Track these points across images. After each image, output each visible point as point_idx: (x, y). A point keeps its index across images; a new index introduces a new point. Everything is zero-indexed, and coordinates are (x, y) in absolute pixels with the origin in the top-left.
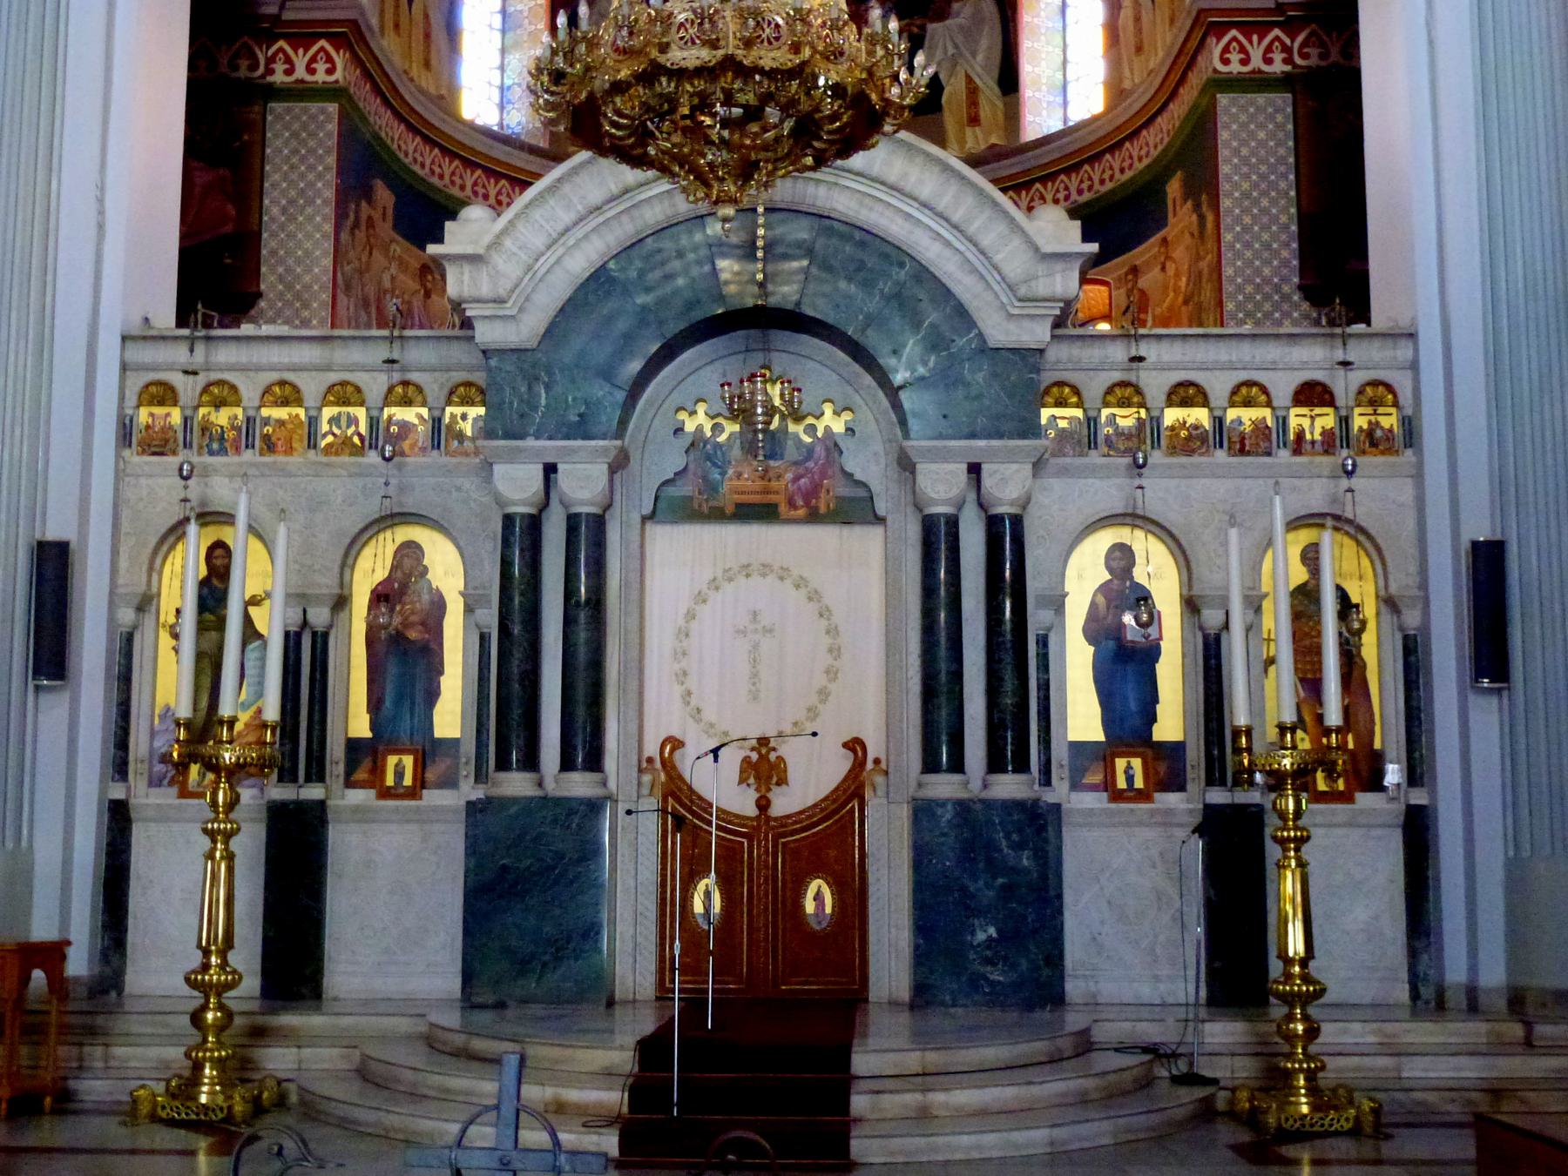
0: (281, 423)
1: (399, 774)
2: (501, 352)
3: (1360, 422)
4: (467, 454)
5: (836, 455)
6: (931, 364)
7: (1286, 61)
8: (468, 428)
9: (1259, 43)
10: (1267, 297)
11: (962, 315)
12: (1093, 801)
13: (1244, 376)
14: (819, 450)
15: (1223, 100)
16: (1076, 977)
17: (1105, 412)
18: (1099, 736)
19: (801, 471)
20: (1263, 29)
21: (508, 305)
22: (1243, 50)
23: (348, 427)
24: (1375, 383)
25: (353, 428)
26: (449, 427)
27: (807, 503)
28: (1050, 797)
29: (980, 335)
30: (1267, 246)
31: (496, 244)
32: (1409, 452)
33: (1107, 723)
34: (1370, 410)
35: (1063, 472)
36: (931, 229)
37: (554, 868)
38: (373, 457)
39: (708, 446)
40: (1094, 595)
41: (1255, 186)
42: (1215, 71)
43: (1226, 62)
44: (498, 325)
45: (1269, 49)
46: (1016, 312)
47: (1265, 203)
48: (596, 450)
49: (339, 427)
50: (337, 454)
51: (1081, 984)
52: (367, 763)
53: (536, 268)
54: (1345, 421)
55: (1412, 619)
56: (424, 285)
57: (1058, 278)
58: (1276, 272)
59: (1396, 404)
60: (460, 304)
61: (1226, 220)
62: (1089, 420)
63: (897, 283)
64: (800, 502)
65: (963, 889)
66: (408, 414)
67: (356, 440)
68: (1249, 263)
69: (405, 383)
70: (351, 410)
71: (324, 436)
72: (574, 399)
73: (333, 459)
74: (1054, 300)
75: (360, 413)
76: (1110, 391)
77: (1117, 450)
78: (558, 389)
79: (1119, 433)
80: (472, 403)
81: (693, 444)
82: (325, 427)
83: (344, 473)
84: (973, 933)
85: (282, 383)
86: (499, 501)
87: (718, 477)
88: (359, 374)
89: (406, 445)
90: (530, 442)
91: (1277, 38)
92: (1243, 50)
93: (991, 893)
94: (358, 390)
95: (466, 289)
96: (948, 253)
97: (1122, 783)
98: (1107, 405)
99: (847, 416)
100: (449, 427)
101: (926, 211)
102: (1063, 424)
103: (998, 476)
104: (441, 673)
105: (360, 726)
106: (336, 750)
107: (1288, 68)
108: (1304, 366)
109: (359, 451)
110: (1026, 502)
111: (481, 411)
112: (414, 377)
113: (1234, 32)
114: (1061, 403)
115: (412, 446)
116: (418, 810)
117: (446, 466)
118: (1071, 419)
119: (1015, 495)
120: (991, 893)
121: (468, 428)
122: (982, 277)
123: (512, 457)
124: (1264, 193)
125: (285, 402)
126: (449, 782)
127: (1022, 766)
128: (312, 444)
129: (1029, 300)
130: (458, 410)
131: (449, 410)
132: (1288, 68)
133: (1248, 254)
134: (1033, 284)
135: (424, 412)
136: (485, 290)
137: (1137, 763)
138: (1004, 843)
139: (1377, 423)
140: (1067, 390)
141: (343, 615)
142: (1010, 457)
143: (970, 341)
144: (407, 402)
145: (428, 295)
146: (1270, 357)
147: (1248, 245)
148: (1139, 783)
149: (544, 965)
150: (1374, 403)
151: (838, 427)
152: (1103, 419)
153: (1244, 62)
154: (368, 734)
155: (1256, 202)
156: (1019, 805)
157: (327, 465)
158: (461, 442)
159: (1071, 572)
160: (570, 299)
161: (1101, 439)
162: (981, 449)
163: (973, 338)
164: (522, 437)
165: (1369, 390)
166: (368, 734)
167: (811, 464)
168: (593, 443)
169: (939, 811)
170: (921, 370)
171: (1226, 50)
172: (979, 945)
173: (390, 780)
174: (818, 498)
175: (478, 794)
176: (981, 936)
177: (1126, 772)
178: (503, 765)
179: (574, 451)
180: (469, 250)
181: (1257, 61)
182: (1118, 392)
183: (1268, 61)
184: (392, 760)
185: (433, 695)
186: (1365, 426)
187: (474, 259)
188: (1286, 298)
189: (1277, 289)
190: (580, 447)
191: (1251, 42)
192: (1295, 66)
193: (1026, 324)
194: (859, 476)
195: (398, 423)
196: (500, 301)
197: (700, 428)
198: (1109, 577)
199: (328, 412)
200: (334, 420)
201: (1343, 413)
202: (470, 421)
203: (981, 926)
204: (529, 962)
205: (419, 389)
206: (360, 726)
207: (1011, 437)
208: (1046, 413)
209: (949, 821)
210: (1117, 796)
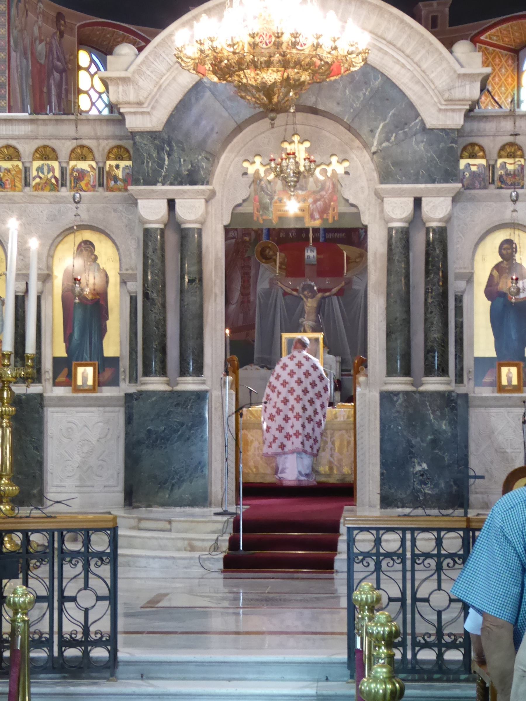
0: (8, 171)
1: (85, 379)
2: (142, 133)
4: (119, 190)
5: (339, 186)
6: (393, 138)
8: (120, 174)
12: (486, 392)
14: (329, 184)
16: (476, 493)
17: (500, 161)
18: (493, 354)
19: (318, 197)
21: (144, 106)
23: (48, 173)
25: (51, 174)
26: (108, 173)
27: (321, 218)
28: (461, 389)
31: (139, 71)
33: (498, 347)
35: (472, 199)
36: (393, 57)
37: (179, 431)
38: (65, 192)
39: (262, 182)
40: (492, 270)
44: (139, 117)
46: (443, 107)
48: (197, 191)
49: (43, 173)
50: (42, 189)
51: (479, 496)
52: (65, 371)
53: (161, 82)
56: (59, 29)
57: (468, 87)
60: (117, 105)
62: (489, 165)
64: (317, 216)
65: (409, 442)
66: (83, 165)
67: (53, 181)
69: (82, 147)
70: (49, 162)
71: (34, 178)
72: (184, 161)
73: (41, 193)
74: (467, 100)
75: (55, 164)
76: (503, 148)
77: (506, 184)
78: (175, 155)
79: (508, 174)
80: (121, 158)
81: (253, 182)
82: (34, 173)
83: (47, 201)
84: (414, 467)
85: (8, 147)
86: (142, 221)
87: (268, 201)
88: (54, 141)
89: (83, 184)
90: (159, 187)
93: (424, 445)
94: (54, 150)
95: (120, 96)
96: (403, 71)
97: (504, 382)
98: (500, 157)
99: (346, 164)
100: (108, 173)
101: (391, 46)
102: (474, 169)
103: (432, 204)
104: (107, 319)
105: (61, 352)
106: (47, 365)
109: (54, 188)
110: (448, 219)
111: (129, 163)
112: (86, 142)
114: (473, 156)
115: (87, 185)
116: (97, 398)
117: (106, 197)
118: (479, 166)
119: (441, 216)
120: (424, 445)
121: (120, 174)
122: (424, 86)
123: (149, 196)
125: (10, 159)
126: (114, 382)
127: (443, 371)
128: (27, 184)
129: (451, 100)
130: (114, 163)
131: (108, 163)
134: (452, 91)
135: (94, 164)
136: (132, 98)
137: (514, 370)
138: (432, 416)
140: (477, 148)
141: (48, 285)
142: (439, 194)
143: (416, 125)
144: (83, 158)
145: (62, 35)
148: (515, 382)
149: (173, 485)
151: (340, 169)
152: (498, 165)
154: (65, 355)
156: (440, 394)
157: (37, 196)
158: (116, 182)
159: (478, 257)
160: (181, 101)
161: (496, 179)
162: (421, 189)
163: (418, 123)
164: (155, 184)
166: (65, 355)
167: (323, 193)
169: (395, 399)
172: (416, 473)
173: (79, 382)
174: (328, 214)
175: (132, 389)
176: (418, 468)
177: (507, 376)
178: (147, 373)
179: (185, 192)
180: (123, 74)
182: (508, 149)
184: (80, 370)
185: (102, 331)
187: (125, 80)
190: (188, 190)
193: (450, 114)
194: (352, 201)
195: (77, 171)
196: (140, 104)
197: (257, 172)
198: (500, 259)
199: (37, 164)
200: (40, 169)
202: (121, 169)
203: (419, 463)
204: (165, 483)
205: (90, 150)
206: (61, 352)
207: (439, 182)
208: (463, 163)
209: (400, 405)
210: (501, 389)
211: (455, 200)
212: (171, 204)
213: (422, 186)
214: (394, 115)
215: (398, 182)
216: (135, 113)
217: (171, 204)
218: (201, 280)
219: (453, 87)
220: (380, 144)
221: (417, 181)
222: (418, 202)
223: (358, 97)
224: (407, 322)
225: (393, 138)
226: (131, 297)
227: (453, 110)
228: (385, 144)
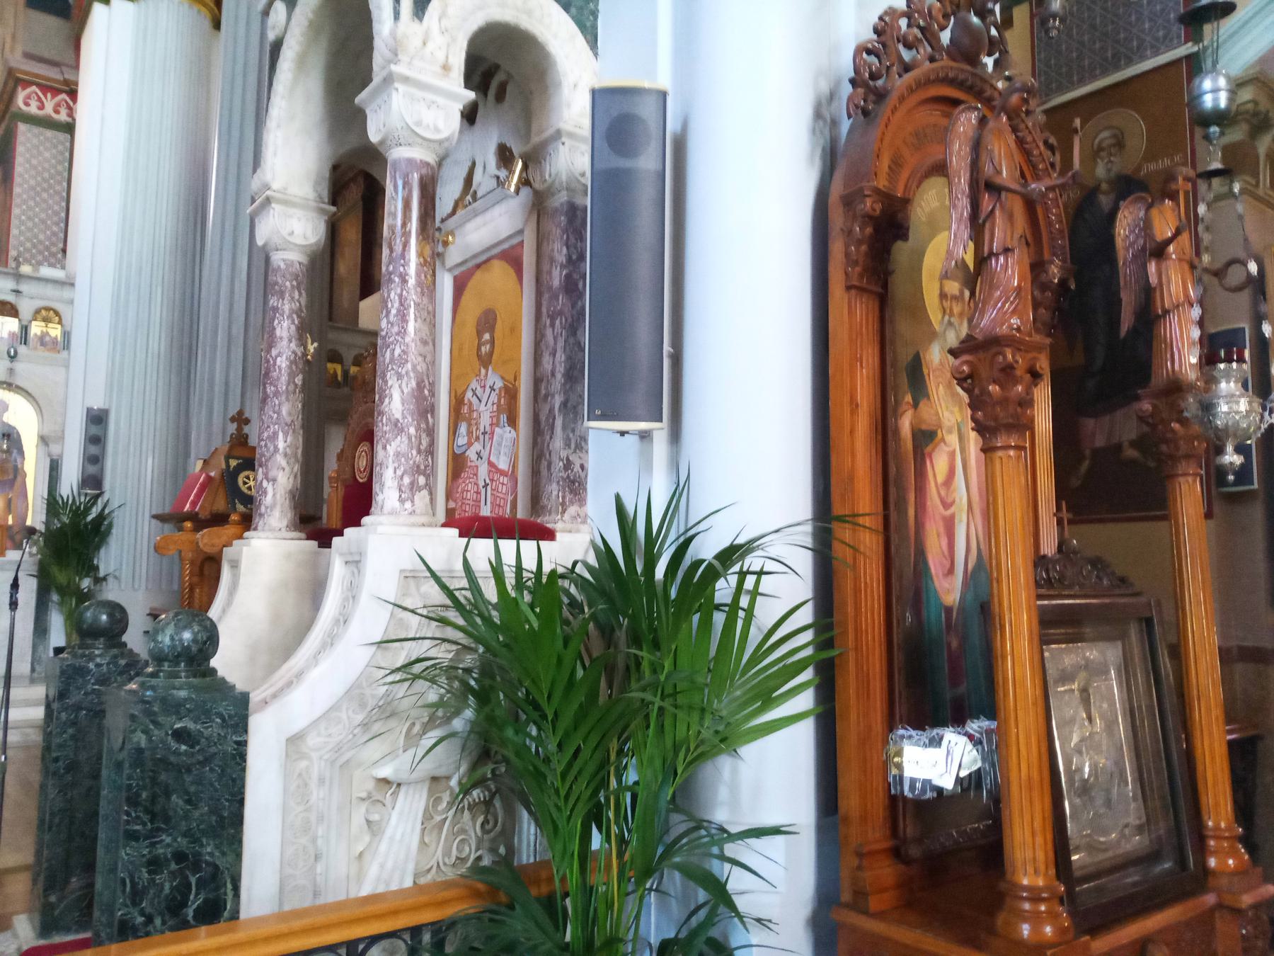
3: (36, 328)
15: (22, 127)
20: (56, 92)
22: (39, 99)
24: (48, 309)
30: (43, 222)
34: (43, 324)
41: (38, 184)
43: (27, 104)
47: (45, 195)
54: (25, 329)
55: (55, 449)
58: (49, 239)
59: (60, 322)
61: (16, 201)
68: (30, 230)
92: (39, 99)
113: (34, 88)
124: (44, 190)
133: (30, 224)
139: (47, 333)
147: (29, 218)
150: (47, 320)
155: (38, 194)
165: (43, 312)
171: (29, 97)
183: (57, 112)
186: (39, 333)
189: (47, 248)
191: (46, 98)
201: (25, 323)
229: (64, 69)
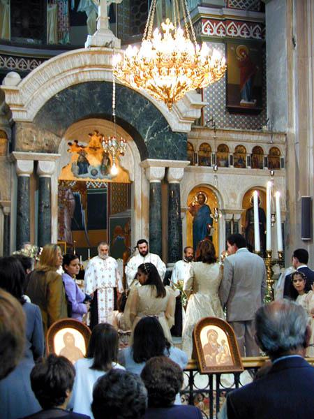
7: (224, 33)
9: (216, 25)
10: (216, 110)
11: (164, 122)
13: (240, 143)
20: (217, 21)
22: (211, 28)
29: (170, 128)
32: (283, 169)
42: (202, 34)
44: (20, 113)
45: (219, 28)
63: (145, 109)
91: (221, 25)
107: (224, 35)
108: (256, 142)
113: (208, 21)
132: (224, 35)
136: (18, 102)
142: (178, 166)
146: (246, 138)
153: (212, 32)
168: (52, 154)
170: (151, 138)
171: (206, 27)
179: (44, 156)
181: (215, 32)
187: (16, 91)
188: (222, 110)
192: (227, 35)
193: (184, 125)
196: (22, 106)
211: (186, 170)
212: (36, 163)
213: (171, 161)
214: (156, 123)
215: (158, 158)
216: (18, 111)
217: (36, 163)
218: (51, 208)
219: (188, 111)
220: (149, 138)
221: (167, 159)
222: (167, 169)
223: (138, 112)
224: (9, 237)
225: (155, 135)
226: (5, 216)
227: (186, 123)
228: (151, 138)
229: (223, 9)
